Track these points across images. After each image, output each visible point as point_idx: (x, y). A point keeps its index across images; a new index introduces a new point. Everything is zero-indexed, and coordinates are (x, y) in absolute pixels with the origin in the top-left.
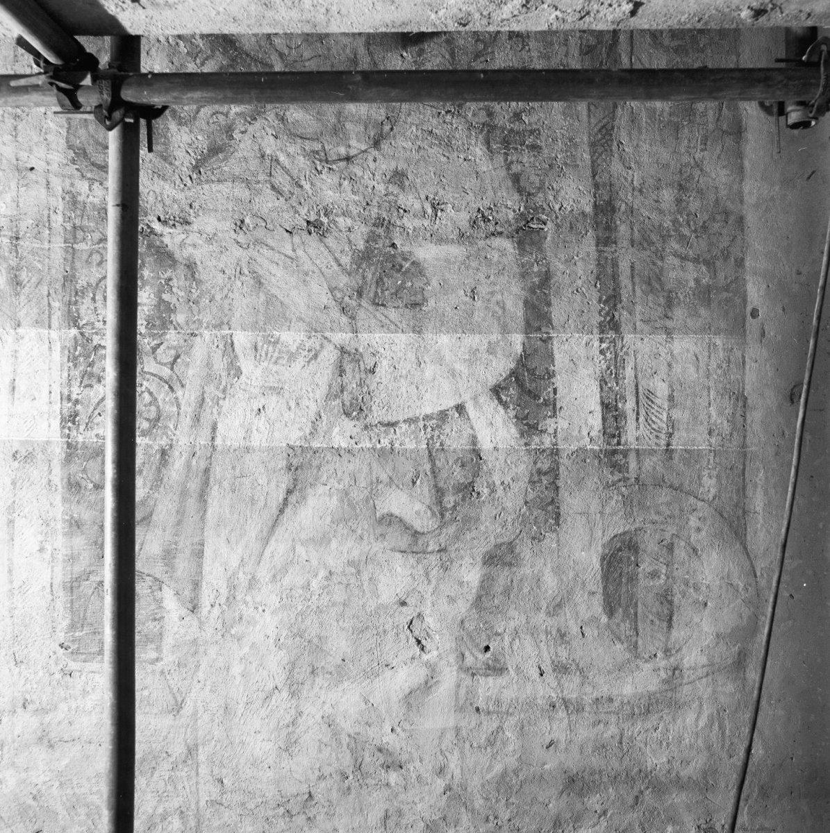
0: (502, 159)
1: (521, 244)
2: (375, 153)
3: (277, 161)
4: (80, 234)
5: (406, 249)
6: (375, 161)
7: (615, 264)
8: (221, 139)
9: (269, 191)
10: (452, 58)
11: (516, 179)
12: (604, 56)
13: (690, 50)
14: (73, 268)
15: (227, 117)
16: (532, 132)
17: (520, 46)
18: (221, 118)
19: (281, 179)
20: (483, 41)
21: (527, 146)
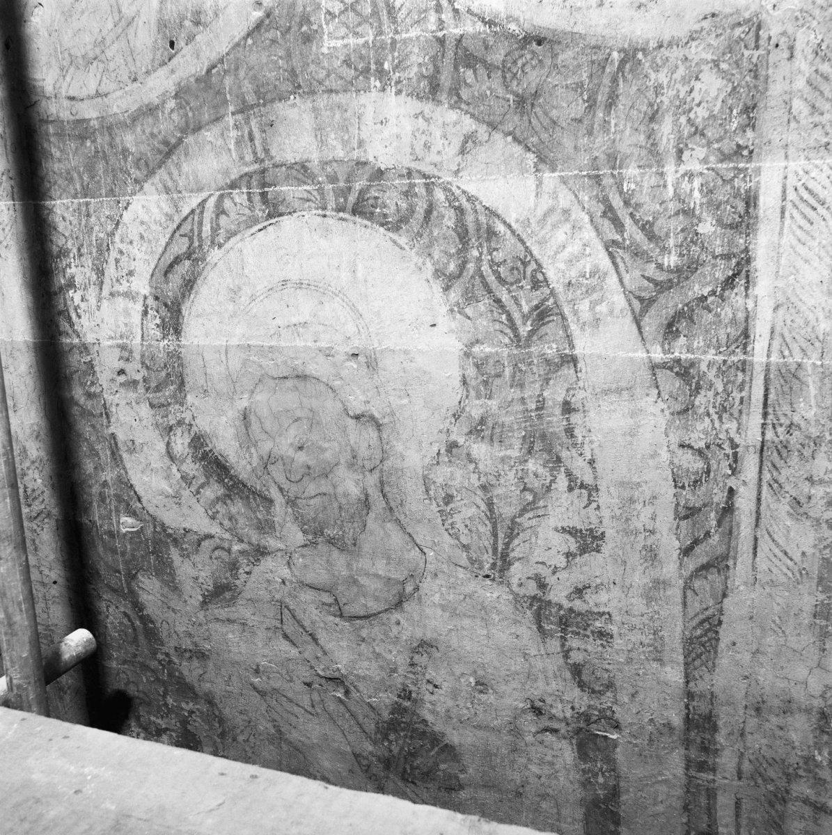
1: (583, 751)
7: (711, 794)
8: (225, 578)
10: (490, 511)
11: (577, 670)
12: (714, 523)
15: (229, 553)
17: (586, 499)
18: (224, 555)
20: (531, 490)
21: (593, 632)
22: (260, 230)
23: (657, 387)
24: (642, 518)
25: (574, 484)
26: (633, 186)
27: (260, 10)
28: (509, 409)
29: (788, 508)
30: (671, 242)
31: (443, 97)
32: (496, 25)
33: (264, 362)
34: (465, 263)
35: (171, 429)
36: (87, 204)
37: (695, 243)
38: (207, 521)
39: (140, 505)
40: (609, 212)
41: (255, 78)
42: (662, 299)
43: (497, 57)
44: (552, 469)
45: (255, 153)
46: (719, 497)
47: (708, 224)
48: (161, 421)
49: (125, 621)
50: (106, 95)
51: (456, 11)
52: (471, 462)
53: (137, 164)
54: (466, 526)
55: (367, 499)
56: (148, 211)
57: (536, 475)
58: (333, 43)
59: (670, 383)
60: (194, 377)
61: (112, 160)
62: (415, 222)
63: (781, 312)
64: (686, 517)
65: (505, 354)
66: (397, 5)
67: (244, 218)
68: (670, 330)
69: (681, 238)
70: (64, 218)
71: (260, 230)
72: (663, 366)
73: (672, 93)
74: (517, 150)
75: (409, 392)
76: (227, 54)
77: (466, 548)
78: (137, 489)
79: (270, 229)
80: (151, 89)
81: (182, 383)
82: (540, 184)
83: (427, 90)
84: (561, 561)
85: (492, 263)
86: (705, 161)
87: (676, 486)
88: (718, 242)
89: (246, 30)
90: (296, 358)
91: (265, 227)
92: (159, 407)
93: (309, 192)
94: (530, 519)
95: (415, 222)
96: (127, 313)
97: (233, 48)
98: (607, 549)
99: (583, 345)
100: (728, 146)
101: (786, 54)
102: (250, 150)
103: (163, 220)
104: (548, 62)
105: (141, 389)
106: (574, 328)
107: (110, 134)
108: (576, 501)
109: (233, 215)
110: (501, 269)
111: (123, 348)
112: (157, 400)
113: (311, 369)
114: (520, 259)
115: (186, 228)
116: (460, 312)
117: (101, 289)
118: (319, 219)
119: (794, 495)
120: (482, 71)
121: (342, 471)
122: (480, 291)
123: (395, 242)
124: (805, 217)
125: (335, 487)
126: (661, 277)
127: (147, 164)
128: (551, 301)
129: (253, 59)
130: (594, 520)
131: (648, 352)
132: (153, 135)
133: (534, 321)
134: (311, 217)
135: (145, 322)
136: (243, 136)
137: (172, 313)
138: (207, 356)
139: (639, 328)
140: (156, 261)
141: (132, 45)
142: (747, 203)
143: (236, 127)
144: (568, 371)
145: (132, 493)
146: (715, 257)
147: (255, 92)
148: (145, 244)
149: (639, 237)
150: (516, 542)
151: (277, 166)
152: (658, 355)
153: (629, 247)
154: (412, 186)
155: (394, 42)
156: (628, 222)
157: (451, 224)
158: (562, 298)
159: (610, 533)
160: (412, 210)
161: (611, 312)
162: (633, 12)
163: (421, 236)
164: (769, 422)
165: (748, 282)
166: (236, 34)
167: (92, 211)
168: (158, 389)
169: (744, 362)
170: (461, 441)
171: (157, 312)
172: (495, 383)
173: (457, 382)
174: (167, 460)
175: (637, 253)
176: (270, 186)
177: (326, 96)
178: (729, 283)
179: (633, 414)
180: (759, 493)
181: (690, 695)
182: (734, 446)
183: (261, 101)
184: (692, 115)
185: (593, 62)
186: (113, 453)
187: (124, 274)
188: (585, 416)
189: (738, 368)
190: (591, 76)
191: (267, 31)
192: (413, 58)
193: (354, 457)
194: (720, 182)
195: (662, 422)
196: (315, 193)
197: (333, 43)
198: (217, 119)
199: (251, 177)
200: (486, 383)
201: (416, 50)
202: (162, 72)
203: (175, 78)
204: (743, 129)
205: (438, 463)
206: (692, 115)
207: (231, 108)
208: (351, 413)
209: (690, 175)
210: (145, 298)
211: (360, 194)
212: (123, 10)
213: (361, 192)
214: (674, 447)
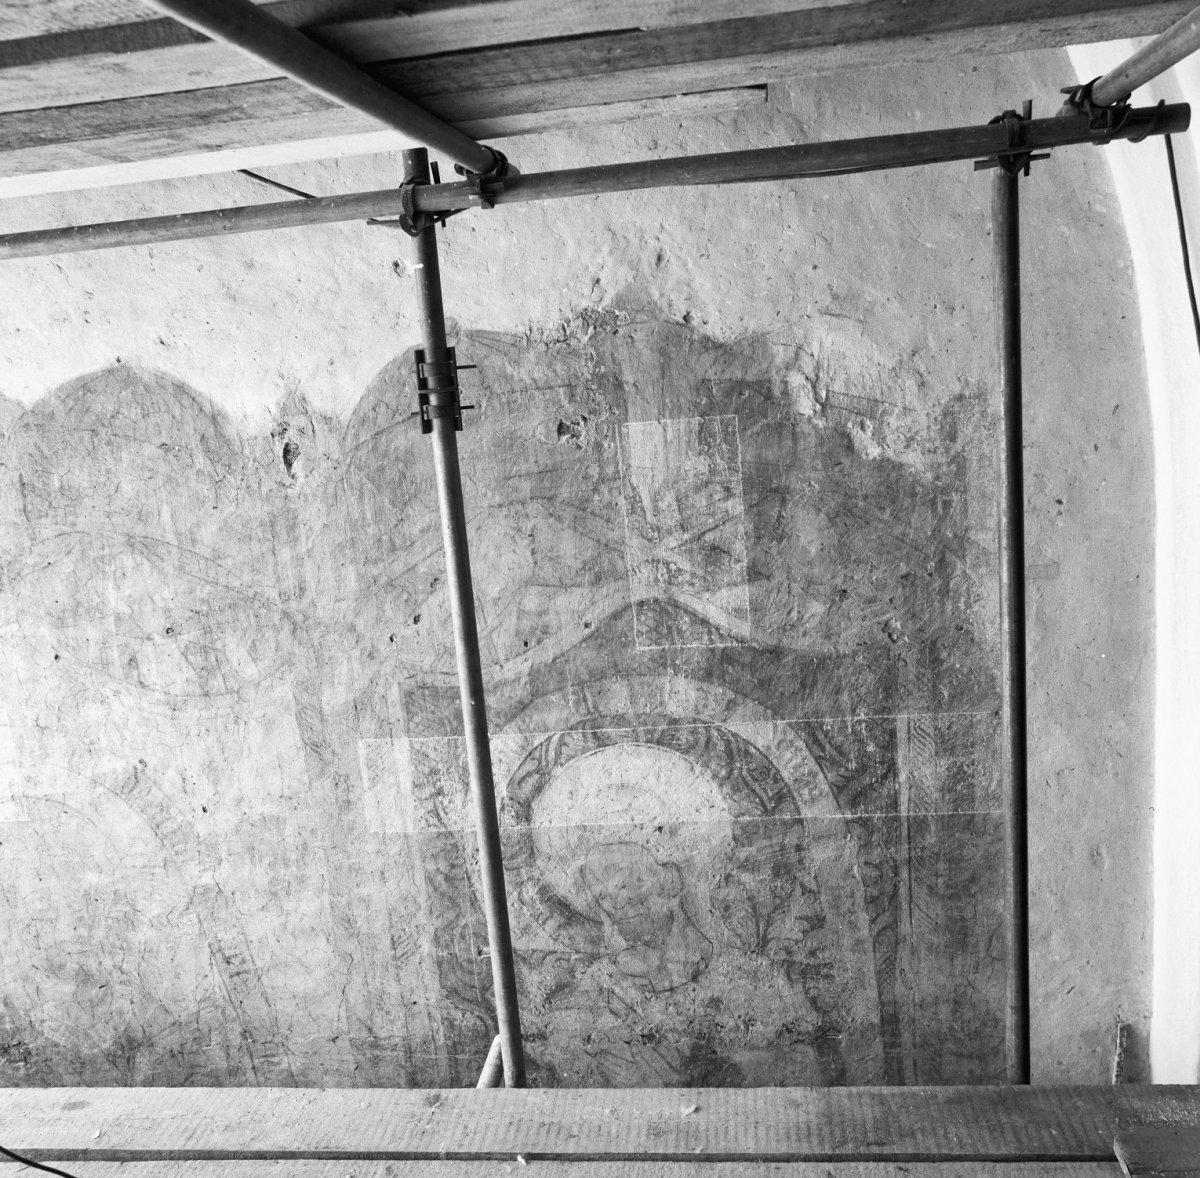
0: (800, 986)
1: (820, 1050)
2: (693, 985)
3: (613, 992)
4: (459, 1047)
5: (725, 1054)
6: (694, 990)
7: (900, 1061)
8: (565, 978)
9: (608, 1014)
11: (814, 1001)
14: (457, 1072)
16: (825, 965)
18: (564, 963)
19: (616, 1005)
25: (805, 890)
34: (732, 770)
36: (456, 740)
38: (552, 941)
40: (816, 741)
43: (747, 659)
45: (588, 709)
46: (889, 889)
49: (479, 1023)
51: (721, 636)
58: (642, 648)
60: (543, 844)
70: (435, 749)
74: (761, 709)
77: (739, 936)
81: (532, 853)
84: (800, 936)
85: (749, 770)
98: (827, 925)
103: (519, 750)
115: (537, 754)
122: (741, 786)
126: (847, 774)
127: (506, 715)
132: (510, 697)
134: (628, 747)
138: (552, 835)
149: (835, 753)
152: (849, 816)
155: (682, 649)
156: (828, 747)
157: (722, 748)
158: (792, 787)
159: (829, 917)
160: (696, 742)
161: (821, 794)
173: (730, 839)
175: (833, 762)
178: (885, 777)
181: (882, 1004)
182: (895, 861)
186: (472, 904)
190: (802, 671)
197: (642, 648)
198: (560, 689)
202: (519, 660)
203: (528, 665)
204: (886, 699)
209: (860, 722)
213: (663, 732)
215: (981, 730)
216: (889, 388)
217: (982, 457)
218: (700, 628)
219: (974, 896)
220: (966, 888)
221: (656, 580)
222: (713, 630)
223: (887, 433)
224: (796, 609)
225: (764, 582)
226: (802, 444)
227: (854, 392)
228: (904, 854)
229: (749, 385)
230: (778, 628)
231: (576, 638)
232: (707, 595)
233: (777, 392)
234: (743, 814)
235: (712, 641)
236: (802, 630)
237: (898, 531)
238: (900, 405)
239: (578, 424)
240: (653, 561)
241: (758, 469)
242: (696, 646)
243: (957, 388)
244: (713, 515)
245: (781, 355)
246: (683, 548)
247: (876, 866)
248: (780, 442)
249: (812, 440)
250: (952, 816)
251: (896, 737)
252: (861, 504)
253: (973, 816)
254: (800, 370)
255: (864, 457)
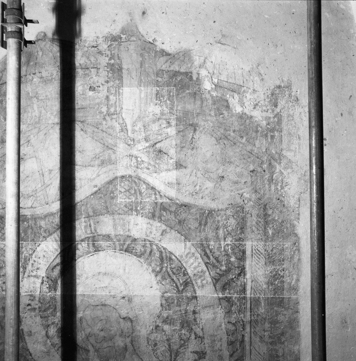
12: (239, 346)
13: (278, 343)
20: (183, 340)
22: (91, 256)
23: (221, 305)
24: (218, 346)
25: (197, 337)
26: (212, 247)
27: (96, 188)
28: (176, 313)
29: (259, 339)
30: (223, 263)
31: (156, 219)
32: (173, 200)
33: (90, 300)
35: (49, 326)
37: (230, 263)
39: (30, 357)
40: (206, 254)
41: (93, 208)
42: (222, 279)
43: (173, 209)
44: (190, 332)
45: (91, 231)
46: (240, 337)
47: (233, 258)
48: (45, 323)
50: (35, 208)
51: (161, 195)
52: (163, 331)
53: (45, 231)
54: (161, 354)
55: (126, 347)
56: (48, 247)
57: (184, 334)
58: (121, 200)
59: (224, 303)
61: (35, 229)
62: (146, 255)
63: (253, 283)
64: (231, 345)
65: (175, 296)
66: (143, 191)
67: (86, 251)
68: (224, 288)
69: (226, 262)
71: (91, 256)
72: (222, 298)
73: (222, 223)
74: (179, 235)
75: (143, 309)
76: (84, 199)
78: (30, 351)
79: (95, 255)
80: (53, 208)
82: (186, 245)
83: (151, 216)
85: (171, 268)
86: (231, 241)
87: (227, 335)
88: (236, 263)
89: (91, 193)
90: (102, 299)
91: (93, 255)
92: (45, 318)
93: (110, 244)
94: (183, 349)
95: (146, 255)
96: (34, 283)
97: (86, 198)
98: (207, 357)
99: (199, 293)
100: (237, 237)
101: (250, 215)
102: (89, 230)
103: (54, 250)
104: (188, 212)
105: (37, 311)
106: (196, 287)
107: (35, 221)
108: (197, 342)
109: (81, 250)
110: (174, 270)
111: (31, 296)
112: (44, 315)
113: (108, 302)
114: (180, 267)
116: (160, 283)
117: (24, 274)
118: (113, 253)
119: (260, 335)
120: (168, 212)
121: (117, 338)
122: (167, 276)
123: (139, 261)
124: (258, 257)
125: (114, 343)
126: (221, 273)
127: (49, 232)
128: (189, 279)
129: (93, 202)
130: (203, 348)
131: (218, 294)
132: (52, 222)
133: (184, 285)
134: (110, 252)
135: (42, 286)
136: (87, 225)
137: (53, 283)
139: (215, 287)
140: (49, 265)
141: (47, 193)
142: (243, 253)
143: (85, 222)
144: (194, 301)
145: (28, 352)
146: (235, 267)
147: (93, 212)
148: (45, 259)
149: (215, 261)
150: (178, 358)
151: (99, 235)
152: (221, 295)
153: (212, 264)
154: (145, 244)
155: (141, 202)
156: (211, 257)
157: (158, 256)
158: (192, 279)
159: (208, 352)
160: (145, 251)
161: (207, 283)
162: (211, 201)
163: (148, 259)
164: (252, 314)
165: (244, 274)
166: (87, 194)
167: (24, 246)
168: (45, 311)
169: (244, 297)
170: (160, 325)
171: (48, 282)
172: (171, 305)
173: (159, 305)
174: (45, 338)
175: (214, 266)
176: (96, 241)
177: (118, 215)
178: (239, 275)
179: (214, 314)
180: (251, 335)
182: (243, 322)
183: (95, 215)
184: (228, 229)
185: (200, 213)
187: (35, 269)
188: (200, 315)
189: (243, 299)
190: (200, 217)
191: (98, 194)
192: (147, 207)
193: (122, 332)
194: (236, 247)
195: (223, 315)
196: (112, 245)
197: (121, 200)
199: (89, 238)
200: (168, 305)
201: (148, 205)
204: (241, 233)
205: (152, 333)
206: (228, 229)
207: (84, 216)
208: (122, 317)
209: (228, 245)
210: (43, 277)
211: (128, 246)
212: (45, 182)
213: (128, 245)
214: (226, 323)
215: (287, 253)
216: (247, 80)
217: (289, 116)
218: (150, 191)
219: (283, 343)
220: (279, 339)
221: (131, 166)
222: (157, 193)
223: (245, 101)
224: (199, 185)
225: (184, 170)
226: (205, 103)
227: (230, 81)
228: (248, 318)
229: (182, 74)
230: (189, 194)
231: (88, 193)
232: (155, 175)
233: (194, 78)
234: (166, 292)
235: (156, 198)
236: (201, 195)
237: (249, 148)
238: (252, 89)
239: (99, 87)
240: (130, 155)
241: (183, 114)
242: (148, 200)
243: (278, 83)
244: (161, 135)
245: (197, 61)
246: (145, 150)
247: (234, 324)
248: (194, 102)
249: (210, 102)
250: (273, 297)
251: (245, 254)
252: (232, 134)
253: (283, 298)
254: (206, 68)
255: (234, 112)
